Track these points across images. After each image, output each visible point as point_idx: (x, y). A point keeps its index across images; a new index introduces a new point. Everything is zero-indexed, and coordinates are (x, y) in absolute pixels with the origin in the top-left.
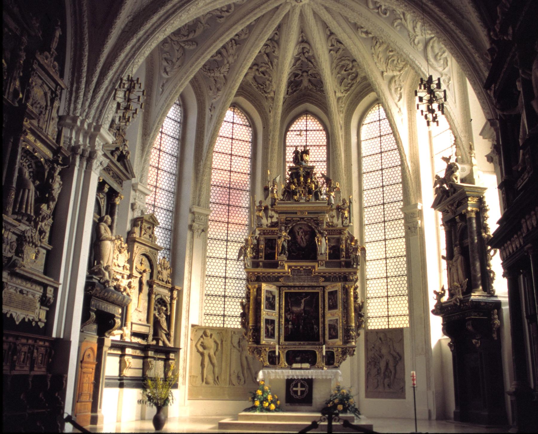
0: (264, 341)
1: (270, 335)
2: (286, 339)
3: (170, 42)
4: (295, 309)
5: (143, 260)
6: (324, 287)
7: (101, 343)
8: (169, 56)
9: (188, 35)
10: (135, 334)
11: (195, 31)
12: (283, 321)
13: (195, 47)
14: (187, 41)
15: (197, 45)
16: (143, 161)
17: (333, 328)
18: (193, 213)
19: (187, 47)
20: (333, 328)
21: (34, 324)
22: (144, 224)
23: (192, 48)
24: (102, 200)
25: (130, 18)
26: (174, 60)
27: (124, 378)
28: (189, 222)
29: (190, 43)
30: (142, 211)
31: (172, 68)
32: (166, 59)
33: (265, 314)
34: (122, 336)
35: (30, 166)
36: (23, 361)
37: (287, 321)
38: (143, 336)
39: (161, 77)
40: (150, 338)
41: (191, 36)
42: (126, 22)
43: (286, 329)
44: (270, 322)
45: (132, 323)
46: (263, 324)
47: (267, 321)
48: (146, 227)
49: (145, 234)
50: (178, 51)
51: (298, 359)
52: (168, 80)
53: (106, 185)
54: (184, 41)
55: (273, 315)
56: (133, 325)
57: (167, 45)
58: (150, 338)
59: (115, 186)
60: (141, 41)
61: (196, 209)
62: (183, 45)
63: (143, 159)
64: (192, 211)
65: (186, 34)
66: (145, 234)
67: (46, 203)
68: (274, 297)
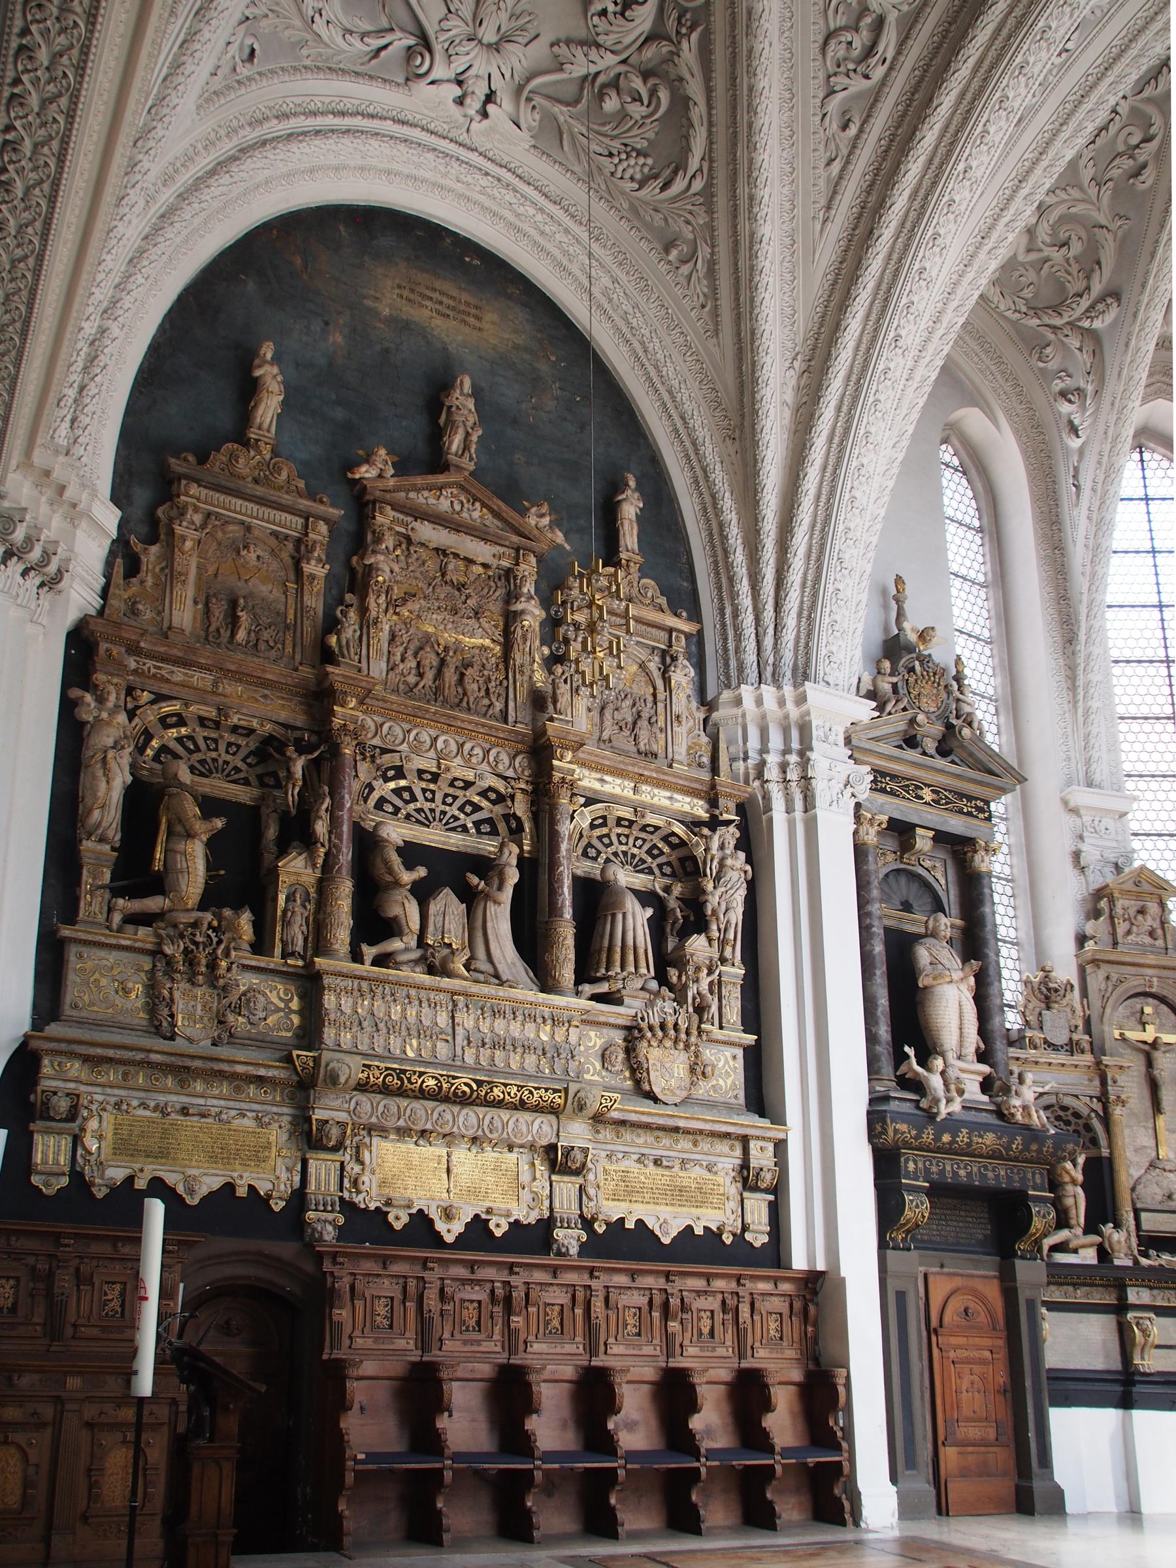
3: (1052, 337)
5: (1148, 1010)
7: (1007, 1280)
8: (1068, 380)
9: (1088, 288)
10: (1151, 1242)
11: (1099, 263)
13: (1113, 312)
14: (1092, 307)
15: (1119, 300)
16: (1081, 720)
18: (1075, 811)
19: (1097, 324)
21: (728, 1239)
22: (1120, 904)
23: (1109, 318)
24: (939, 876)
25: (796, 364)
26: (1082, 385)
27: (1137, 1378)
28: (1069, 846)
29: (1100, 307)
30: (1116, 865)
31: (1083, 408)
32: (1063, 394)
34: (1104, 1254)
35: (655, 852)
36: (712, 1333)
39: (1067, 450)
41: (1097, 288)
42: (794, 382)
45: (1137, 1213)
48: (1132, 912)
49: (1129, 932)
50: (1080, 349)
52: (1081, 451)
53: (919, 831)
54: (1087, 311)
56: (1144, 1216)
57: (1048, 350)
59: (956, 824)
60: (845, 408)
61: (1082, 797)
62: (1086, 324)
63: (1080, 711)
64: (1072, 804)
65: (1079, 286)
66: (1129, 932)
67: (699, 933)
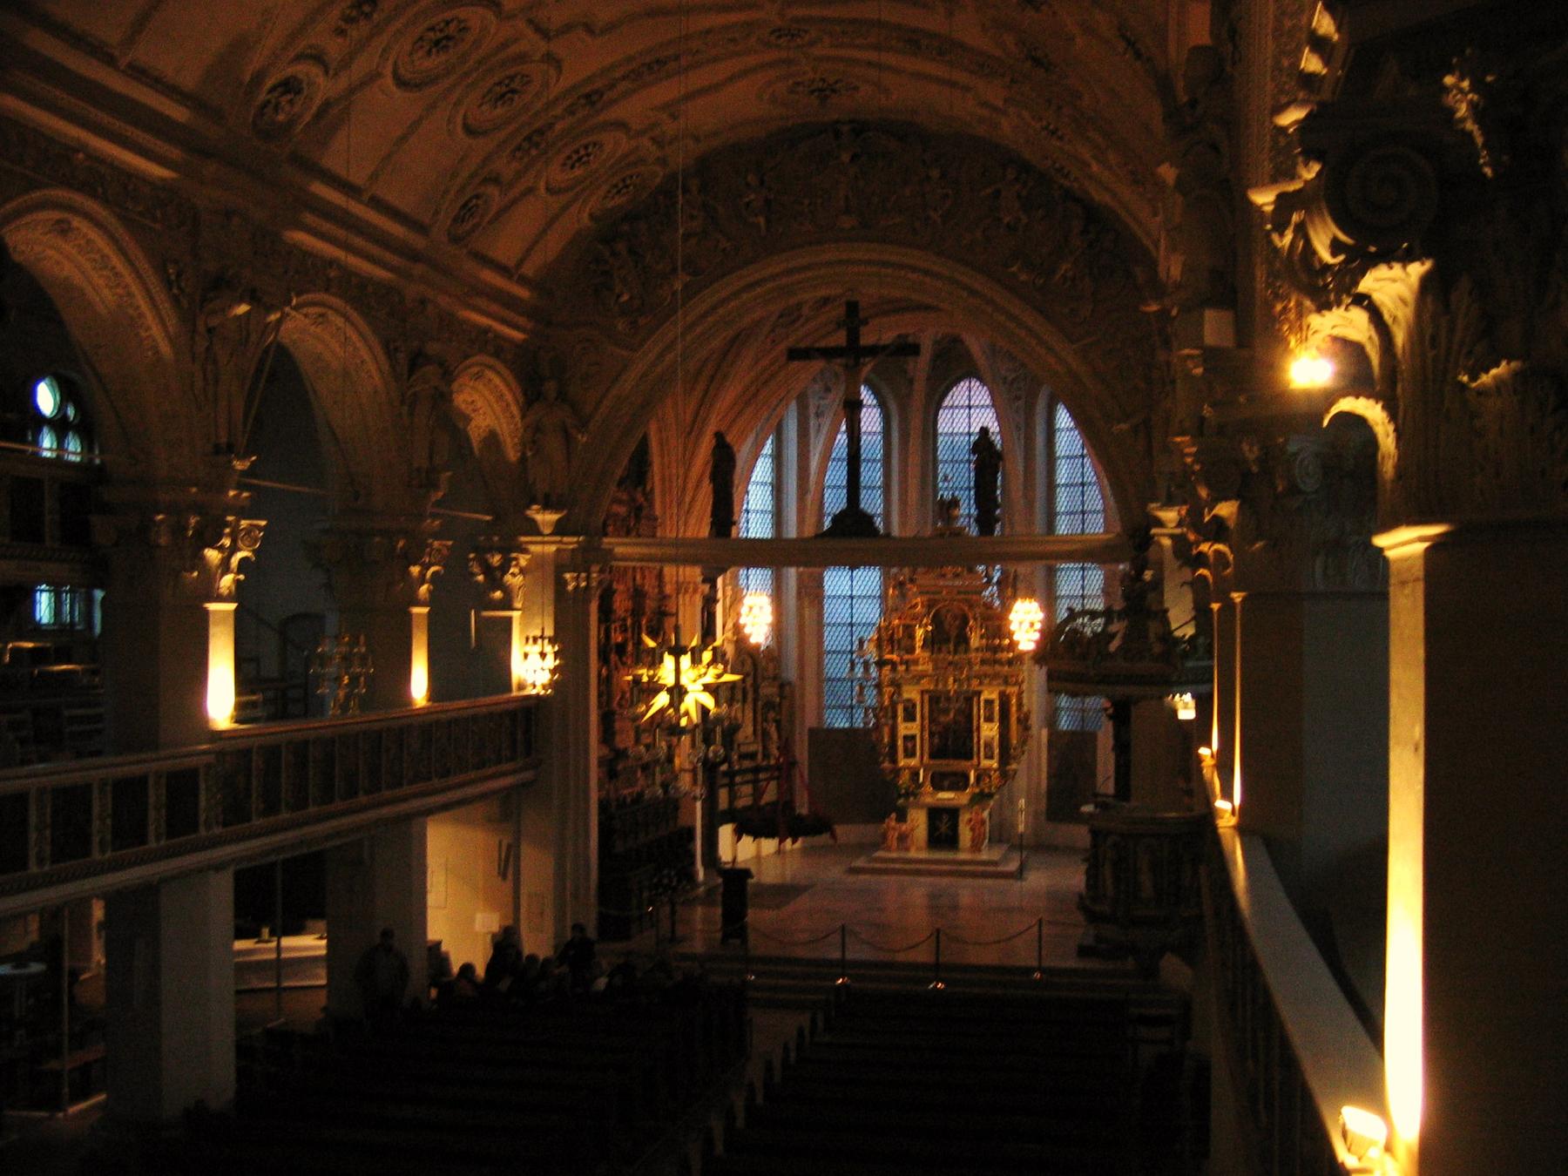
0: (902, 763)
1: (910, 753)
2: (932, 756)
4: (942, 719)
6: (979, 693)
12: (926, 736)
17: (988, 745)
20: (988, 745)
33: (904, 729)
37: (931, 734)
38: (752, 756)
40: (760, 757)
43: (931, 744)
44: (909, 739)
46: (900, 742)
47: (906, 738)
51: (946, 783)
55: (913, 728)
58: (760, 757)
68: (914, 706)
